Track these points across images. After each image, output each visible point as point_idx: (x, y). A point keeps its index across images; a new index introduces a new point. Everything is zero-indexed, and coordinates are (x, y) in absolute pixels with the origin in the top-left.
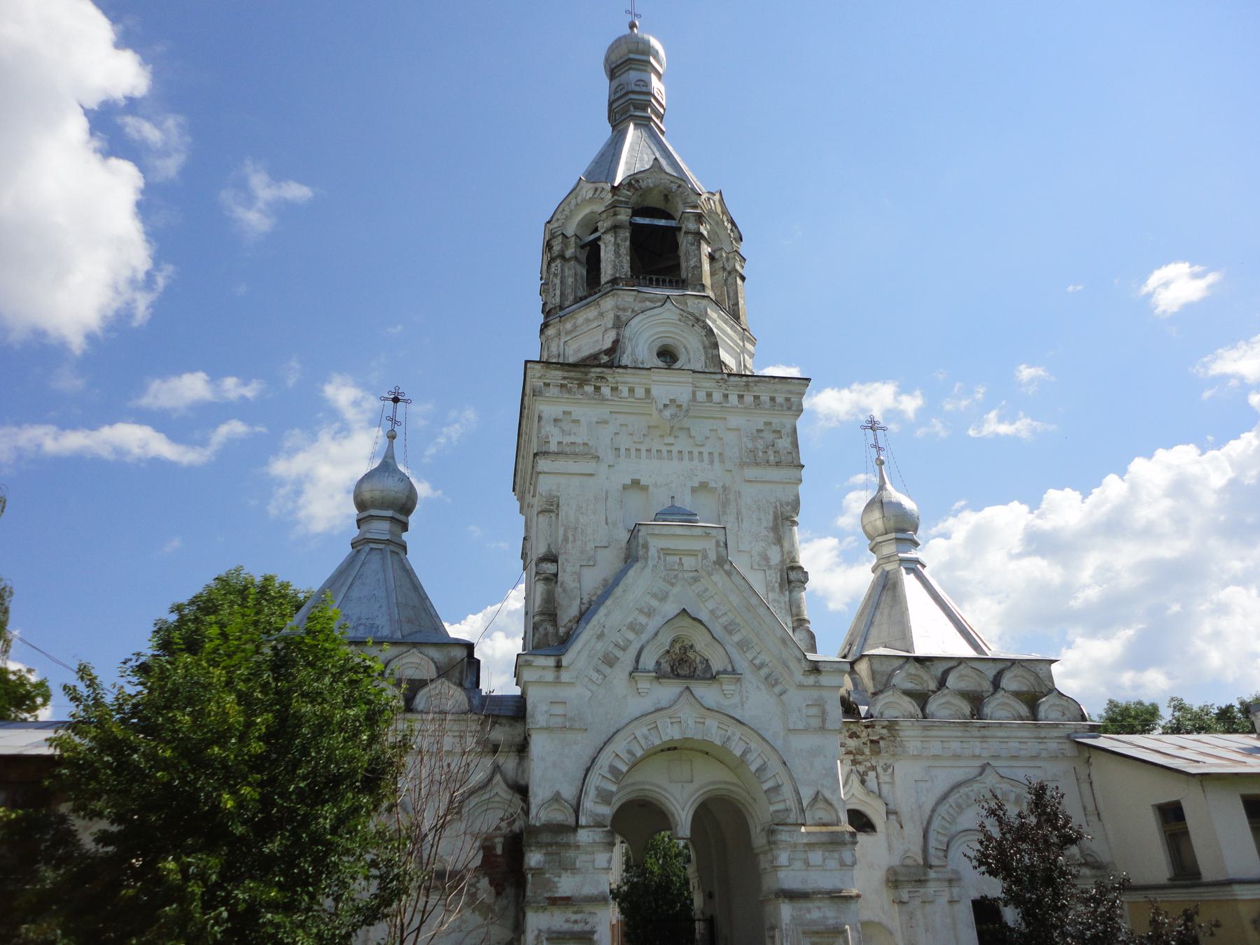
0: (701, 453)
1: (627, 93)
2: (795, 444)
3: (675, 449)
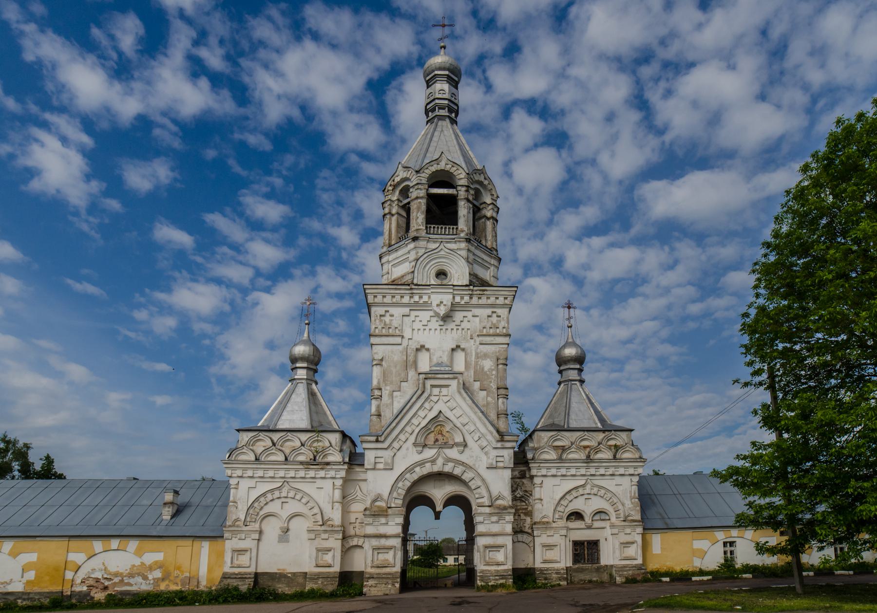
0: (457, 329)
1: (434, 100)
2: (508, 323)
3: (444, 328)
